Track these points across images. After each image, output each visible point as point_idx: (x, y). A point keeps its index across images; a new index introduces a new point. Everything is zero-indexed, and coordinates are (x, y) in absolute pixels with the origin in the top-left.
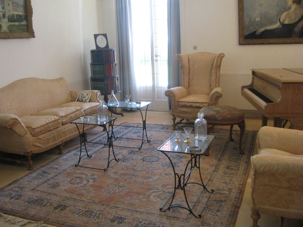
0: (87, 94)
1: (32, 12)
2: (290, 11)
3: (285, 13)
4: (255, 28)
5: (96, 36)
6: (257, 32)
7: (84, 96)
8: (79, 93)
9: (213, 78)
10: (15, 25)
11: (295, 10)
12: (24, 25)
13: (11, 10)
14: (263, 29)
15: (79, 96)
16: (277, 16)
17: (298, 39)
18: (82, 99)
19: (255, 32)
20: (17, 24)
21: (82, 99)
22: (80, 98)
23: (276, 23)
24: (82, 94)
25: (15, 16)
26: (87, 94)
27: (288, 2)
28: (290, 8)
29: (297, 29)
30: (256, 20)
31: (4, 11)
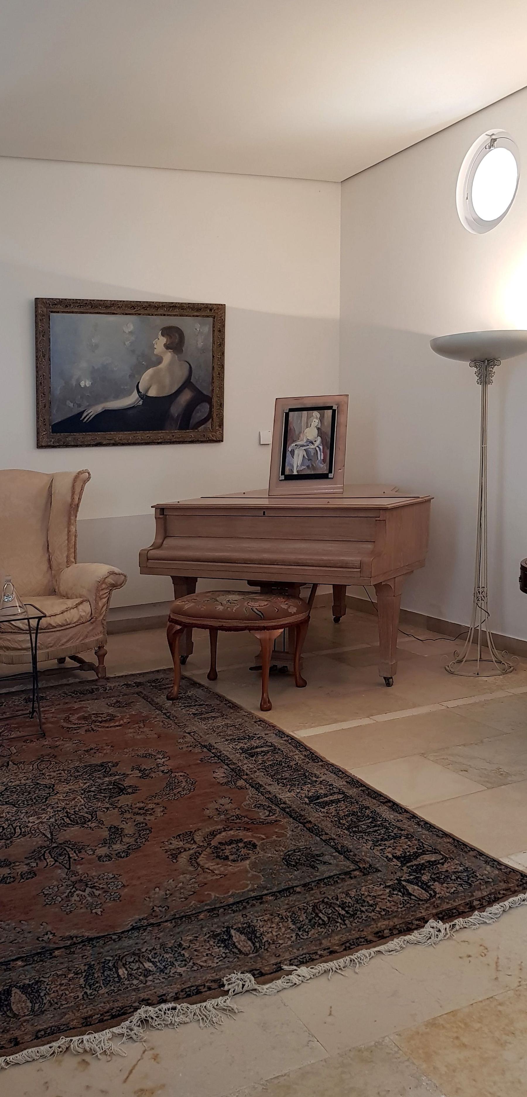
3: (150, 371)
11: (171, 364)
17: (178, 434)
27: (155, 346)
28: (159, 360)
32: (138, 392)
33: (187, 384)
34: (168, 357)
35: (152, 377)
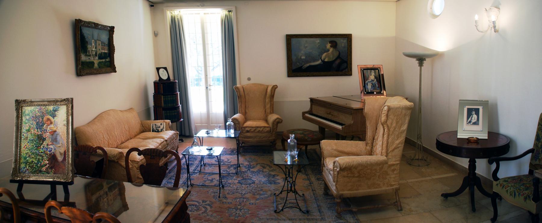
0: (161, 124)
1: (115, 49)
2: (329, 52)
3: (325, 54)
4: (301, 64)
5: (158, 69)
6: (303, 67)
7: (159, 126)
8: (151, 124)
9: (268, 106)
10: (102, 62)
11: (332, 51)
12: (108, 61)
13: (101, 49)
14: (308, 65)
15: (153, 127)
16: (319, 55)
18: (157, 130)
19: (302, 66)
20: (104, 60)
21: (157, 130)
22: (155, 129)
23: (318, 60)
24: (156, 125)
25: (103, 54)
26: (161, 124)
28: (329, 50)
29: (334, 65)
30: (302, 58)
31: (96, 50)
32: (321, 60)
33: (339, 57)
34: (331, 49)
35: (326, 55)
